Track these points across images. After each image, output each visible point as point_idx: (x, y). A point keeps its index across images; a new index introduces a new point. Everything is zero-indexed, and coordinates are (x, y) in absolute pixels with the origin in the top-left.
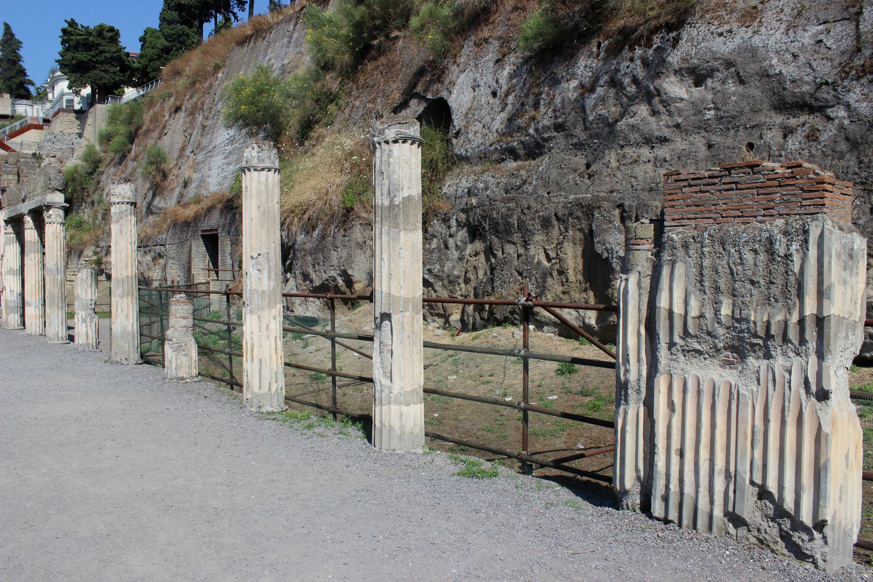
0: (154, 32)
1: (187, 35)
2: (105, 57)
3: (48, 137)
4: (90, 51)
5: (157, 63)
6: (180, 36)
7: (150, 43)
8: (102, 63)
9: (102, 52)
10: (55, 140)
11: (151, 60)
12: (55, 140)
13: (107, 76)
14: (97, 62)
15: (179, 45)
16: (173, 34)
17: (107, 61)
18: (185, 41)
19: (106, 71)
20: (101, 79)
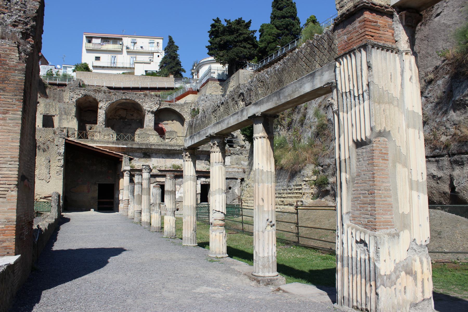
0: (268, 25)
1: (293, 25)
2: (244, 37)
3: (202, 98)
4: (233, 34)
5: (274, 44)
6: (288, 25)
7: (267, 32)
8: (241, 41)
9: (241, 34)
10: (206, 100)
11: (269, 43)
12: (206, 100)
13: (245, 50)
14: (237, 42)
15: (287, 32)
16: (283, 25)
17: (246, 40)
18: (291, 29)
19: (245, 47)
20: (241, 52)
